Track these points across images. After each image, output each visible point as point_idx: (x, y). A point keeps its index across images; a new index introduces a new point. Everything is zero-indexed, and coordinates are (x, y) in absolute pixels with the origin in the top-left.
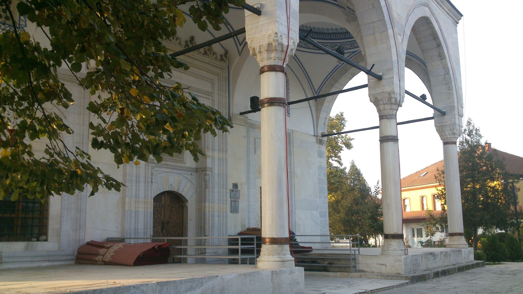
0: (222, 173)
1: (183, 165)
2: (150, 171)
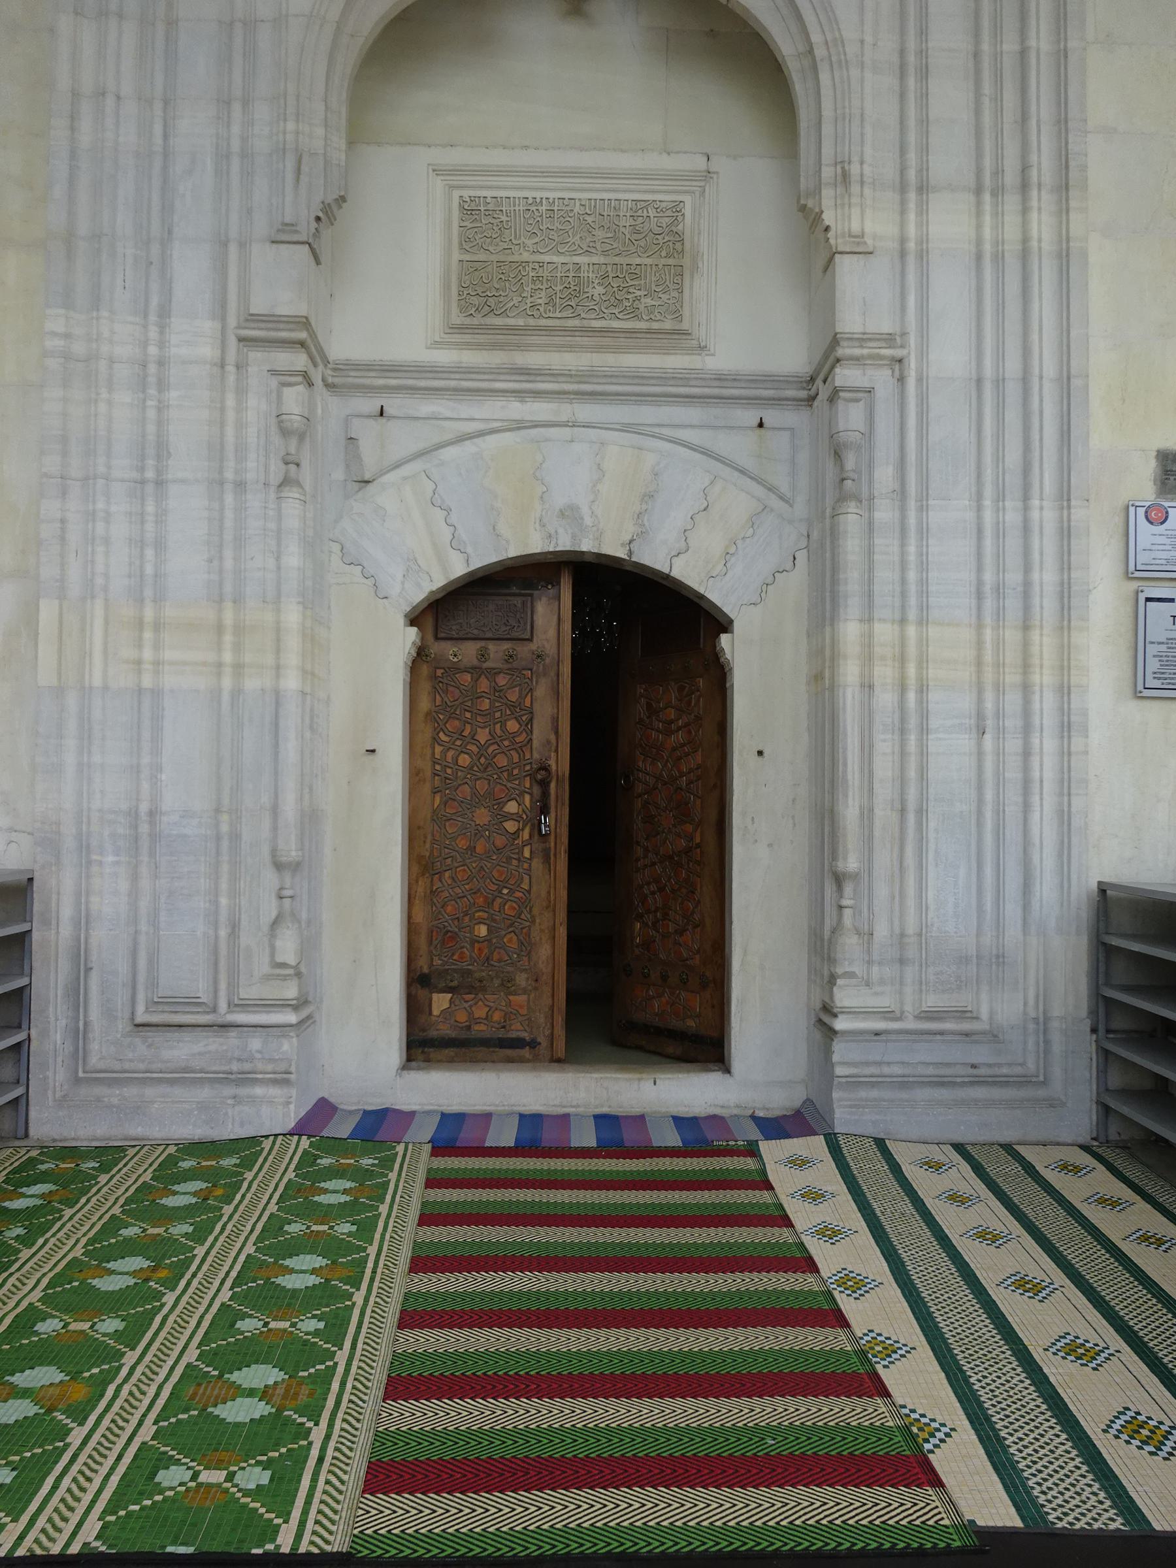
0: (1013, 366)
1: (675, 362)
2: (257, 405)
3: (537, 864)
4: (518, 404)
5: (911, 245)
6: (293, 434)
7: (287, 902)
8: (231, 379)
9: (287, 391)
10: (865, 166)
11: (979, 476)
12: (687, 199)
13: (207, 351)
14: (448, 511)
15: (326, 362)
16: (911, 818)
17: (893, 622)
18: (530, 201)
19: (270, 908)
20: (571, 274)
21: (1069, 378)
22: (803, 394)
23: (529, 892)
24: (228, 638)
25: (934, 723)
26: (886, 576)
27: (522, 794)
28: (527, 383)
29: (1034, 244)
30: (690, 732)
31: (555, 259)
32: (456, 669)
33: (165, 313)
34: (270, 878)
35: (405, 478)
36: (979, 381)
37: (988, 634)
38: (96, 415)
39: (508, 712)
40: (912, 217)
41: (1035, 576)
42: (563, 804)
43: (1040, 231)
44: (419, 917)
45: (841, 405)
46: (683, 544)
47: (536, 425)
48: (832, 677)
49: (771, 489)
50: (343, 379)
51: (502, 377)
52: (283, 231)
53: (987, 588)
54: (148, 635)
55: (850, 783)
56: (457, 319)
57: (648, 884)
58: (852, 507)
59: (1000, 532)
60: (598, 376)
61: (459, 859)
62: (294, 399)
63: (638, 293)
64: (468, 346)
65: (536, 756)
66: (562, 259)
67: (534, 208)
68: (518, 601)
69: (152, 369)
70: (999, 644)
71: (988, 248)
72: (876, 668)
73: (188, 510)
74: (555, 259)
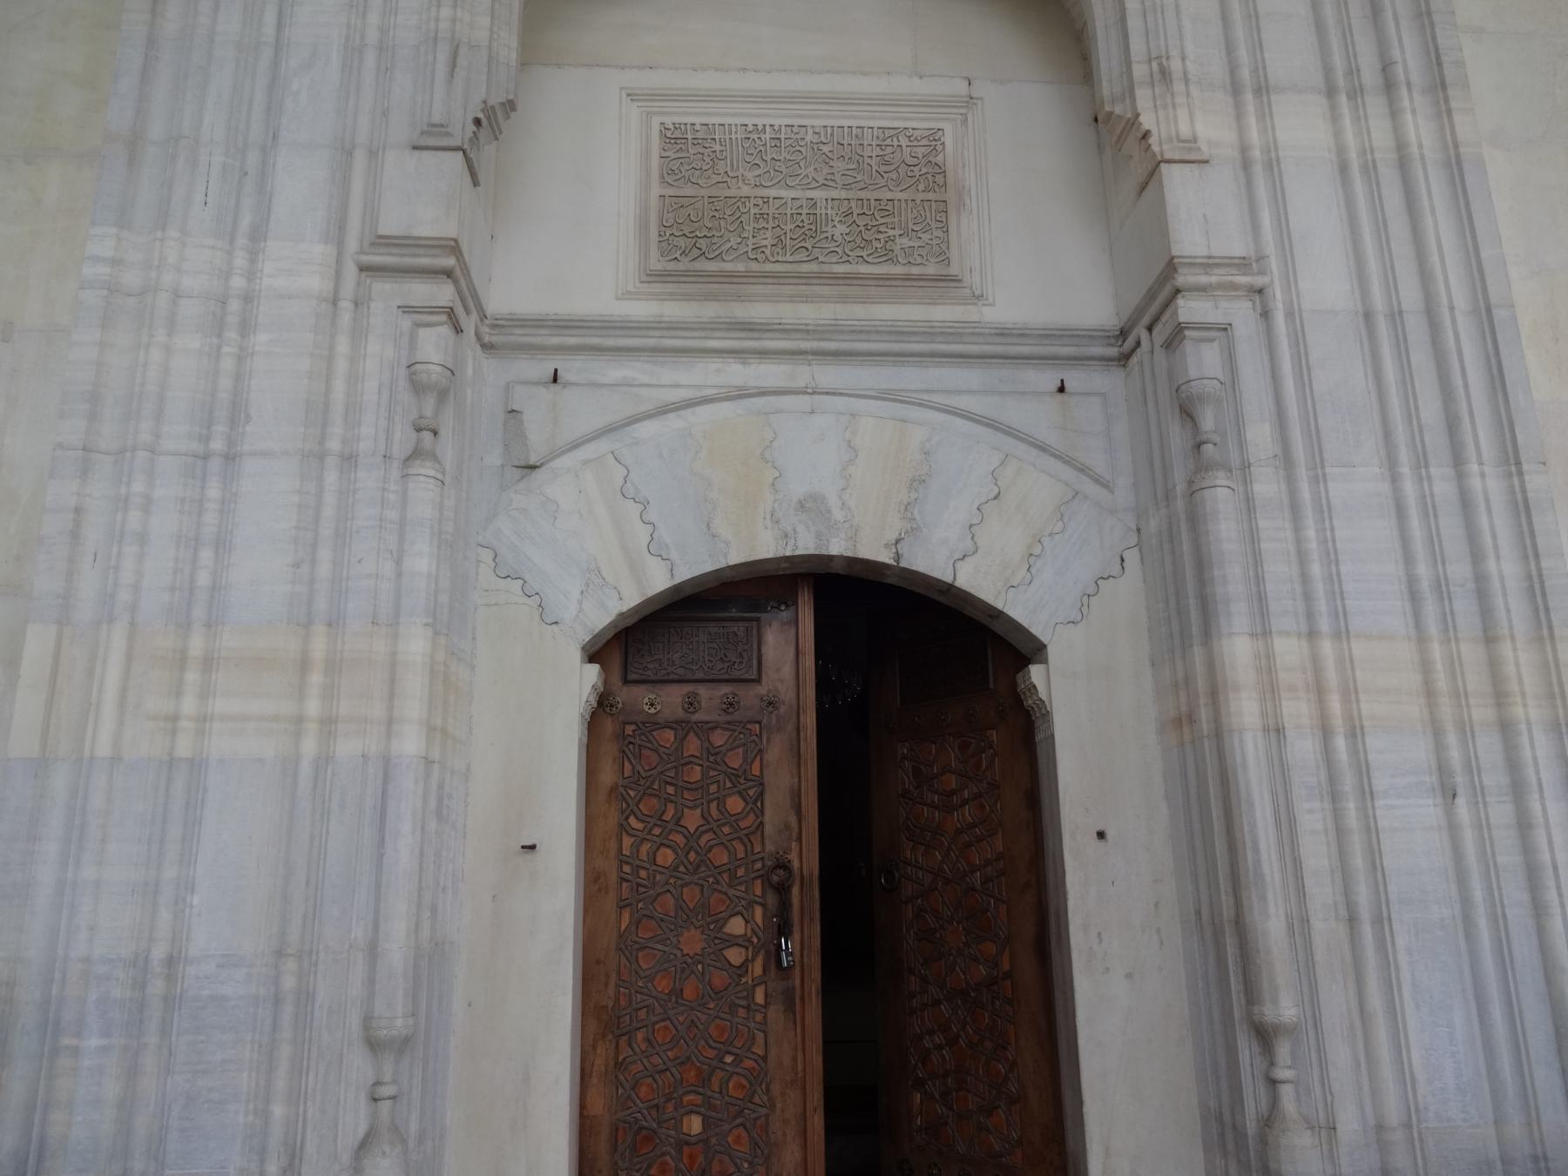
0: (1410, 295)
1: (944, 313)
2: (379, 352)
3: (775, 1014)
4: (740, 367)
5: (1256, 153)
6: (431, 392)
7: (385, 1107)
8: (346, 317)
9: (422, 332)
10: (1188, 63)
11: (1387, 434)
12: (948, 127)
13: (315, 282)
14: (645, 504)
15: (483, 316)
16: (1367, 931)
17: (1299, 635)
18: (750, 128)
19: (354, 1122)
20: (805, 211)
21: (1489, 310)
22: (1113, 352)
23: (765, 1058)
24: (316, 679)
25: (1380, 782)
26: (1279, 571)
27: (751, 904)
28: (750, 340)
29: (1414, 149)
30: (982, 807)
31: (783, 193)
32: (651, 725)
33: (258, 235)
34: (359, 1066)
35: (586, 462)
36: (1368, 316)
37: (1436, 651)
38: (145, 365)
39: (728, 784)
40: (1252, 121)
41: (1491, 565)
42: (812, 919)
43: (1418, 136)
44: (597, 1106)
45: (1188, 347)
46: (969, 543)
47: (763, 393)
48: (1217, 719)
49: (1083, 470)
50: (504, 337)
51: (717, 334)
52: (428, 133)
53: (1425, 585)
54: (192, 676)
55: (1268, 879)
56: (657, 263)
57: (931, 1033)
58: (1221, 478)
59: (1429, 509)
60: (842, 332)
61: (659, 1010)
62: (433, 344)
63: (891, 232)
64: (672, 297)
65: (770, 847)
66: (793, 194)
67: (755, 136)
68: (739, 628)
69: (234, 306)
70: (1454, 666)
71: (1353, 155)
72: (1284, 703)
73: (269, 497)
74: (783, 193)
